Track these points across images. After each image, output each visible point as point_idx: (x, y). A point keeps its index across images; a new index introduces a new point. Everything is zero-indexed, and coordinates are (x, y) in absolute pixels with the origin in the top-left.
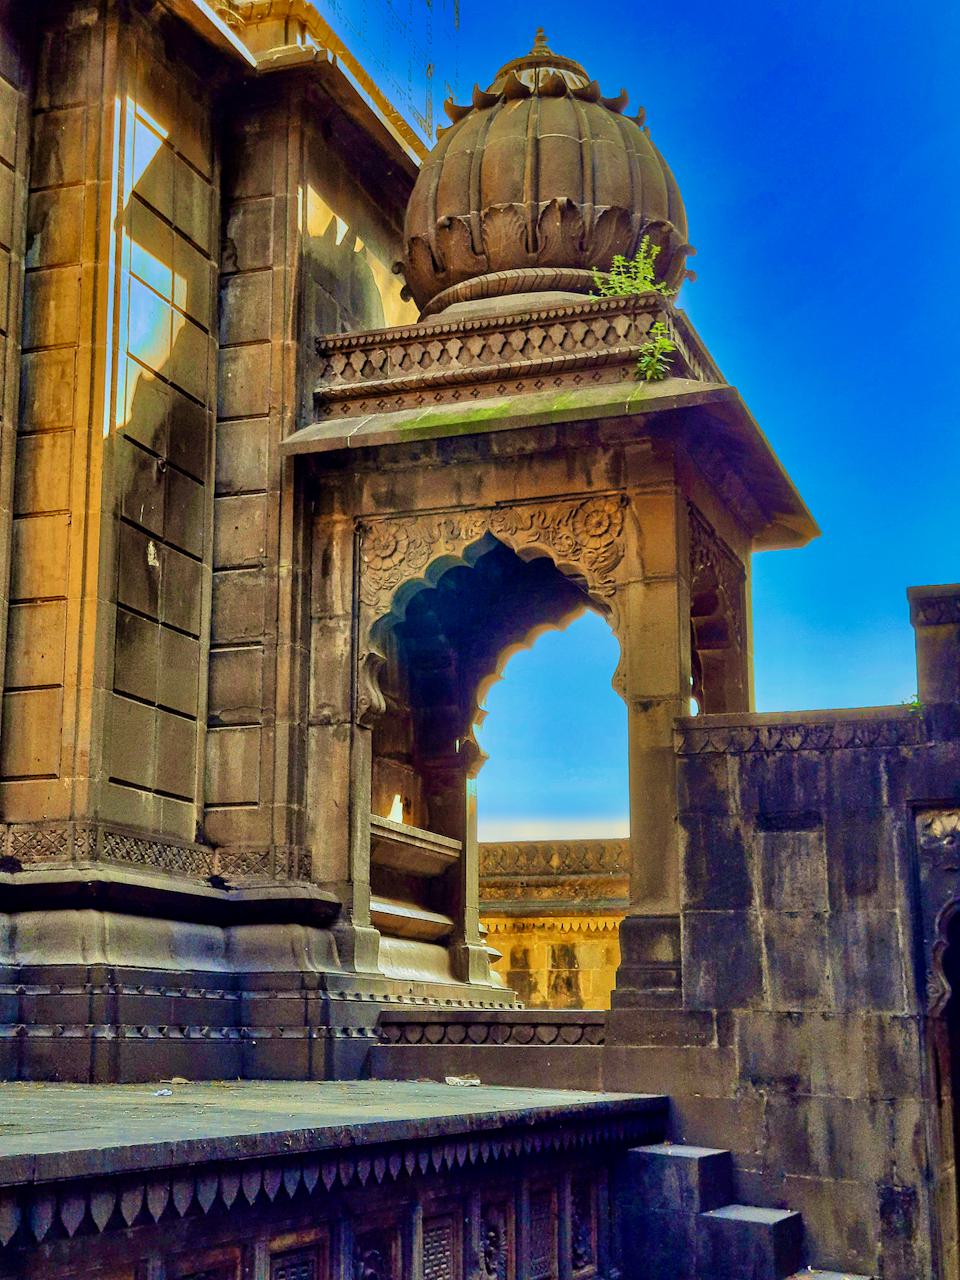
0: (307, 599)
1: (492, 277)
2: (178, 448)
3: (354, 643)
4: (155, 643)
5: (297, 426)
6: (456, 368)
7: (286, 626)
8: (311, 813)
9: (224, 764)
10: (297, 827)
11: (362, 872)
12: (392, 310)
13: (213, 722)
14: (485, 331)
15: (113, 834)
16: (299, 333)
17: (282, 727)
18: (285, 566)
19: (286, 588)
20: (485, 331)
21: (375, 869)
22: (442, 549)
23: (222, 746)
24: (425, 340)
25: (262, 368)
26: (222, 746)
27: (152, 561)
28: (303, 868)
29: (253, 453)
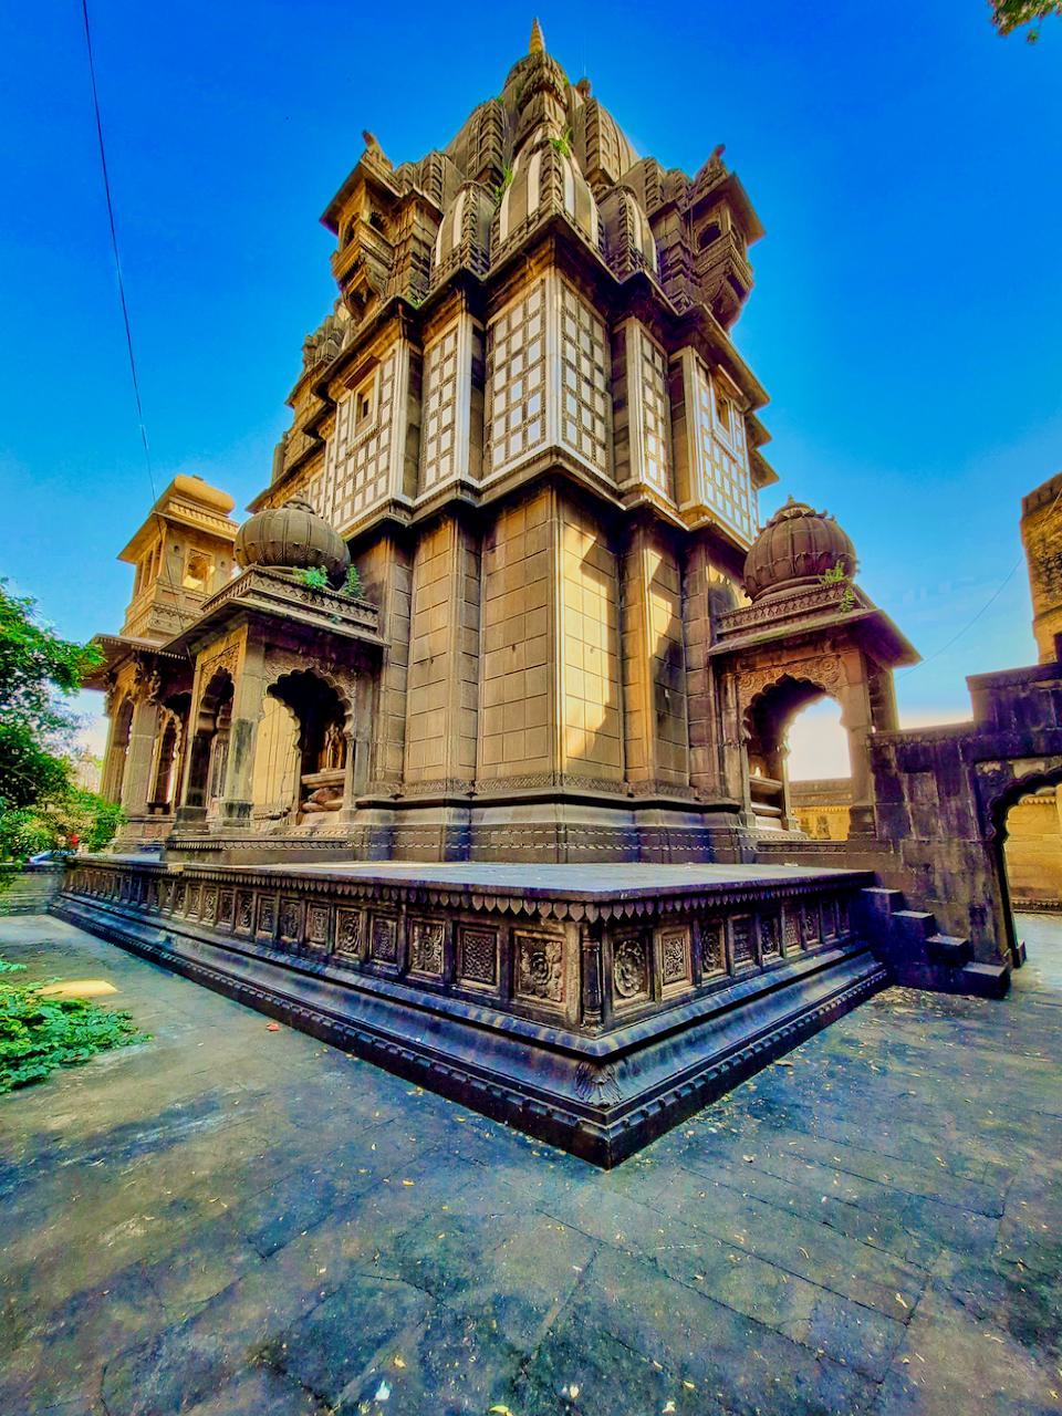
0: (720, 704)
1: (779, 584)
2: (674, 656)
3: (738, 716)
4: (670, 722)
5: (711, 646)
6: (768, 618)
7: (713, 713)
8: (727, 775)
9: (696, 759)
10: (723, 780)
11: (747, 794)
12: (743, 602)
13: (691, 746)
14: (778, 604)
15: (661, 784)
16: (710, 614)
17: (715, 747)
18: (712, 693)
19: (712, 700)
20: (778, 604)
21: (752, 793)
22: (768, 682)
23: (695, 754)
24: (755, 610)
25: (700, 626)
26: (695, 754)
27: (667, 696)
28: (726, 793)
29: (698, 655)
